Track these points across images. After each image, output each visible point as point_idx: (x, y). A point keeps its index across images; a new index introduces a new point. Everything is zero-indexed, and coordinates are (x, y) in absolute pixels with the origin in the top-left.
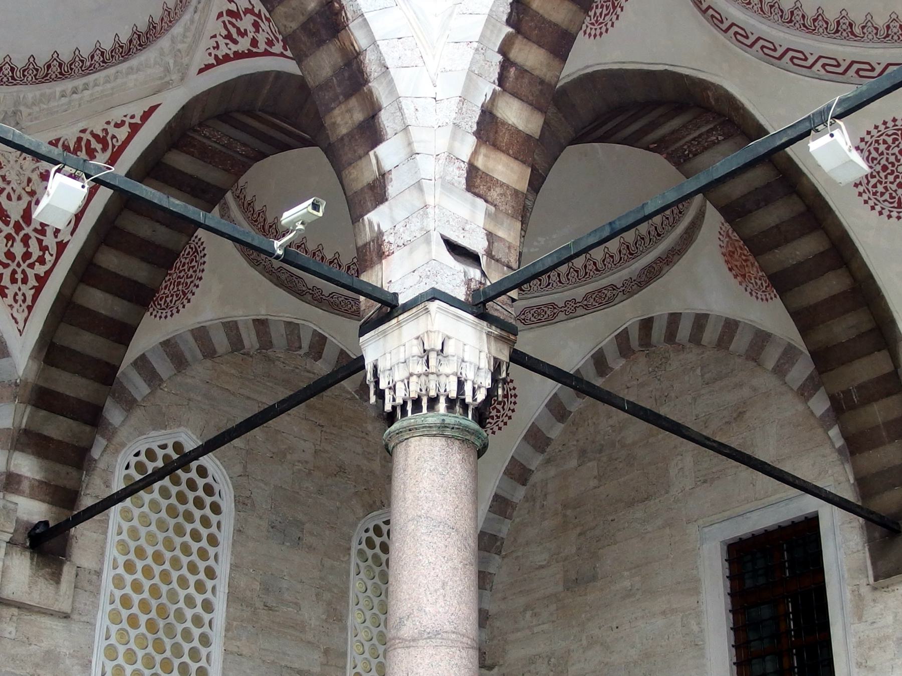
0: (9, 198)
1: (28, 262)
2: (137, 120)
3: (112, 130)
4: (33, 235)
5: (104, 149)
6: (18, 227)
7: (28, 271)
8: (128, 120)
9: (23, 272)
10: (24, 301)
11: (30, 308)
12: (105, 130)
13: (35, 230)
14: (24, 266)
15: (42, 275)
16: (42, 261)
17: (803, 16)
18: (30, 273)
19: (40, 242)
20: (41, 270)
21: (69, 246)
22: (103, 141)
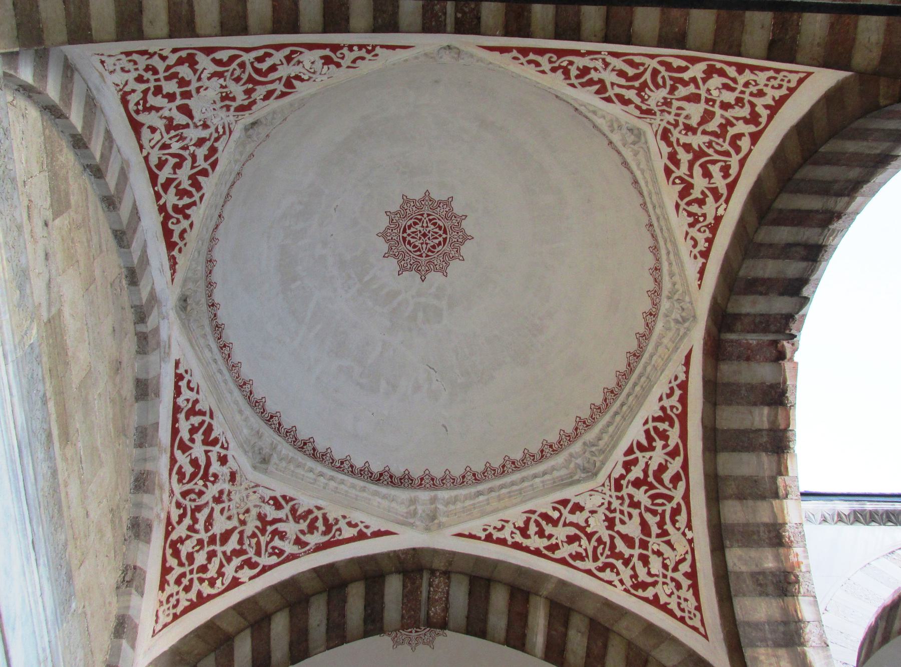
1: (200, 575)
3: (342, 524)
4: (220, 555)
5: (325, 533)
6: (212, 540)
7: (196, 582)
8: (361, 526)
9: (191, 581)
10: (175, 607)
11: (176, 617)
12: (337, 521)
13: (224, 553)
14: (195, 576)
18: (196, 586)
19: (222, 565)
20: (207, 590)
21: (241, 587)
22: (328, 527)
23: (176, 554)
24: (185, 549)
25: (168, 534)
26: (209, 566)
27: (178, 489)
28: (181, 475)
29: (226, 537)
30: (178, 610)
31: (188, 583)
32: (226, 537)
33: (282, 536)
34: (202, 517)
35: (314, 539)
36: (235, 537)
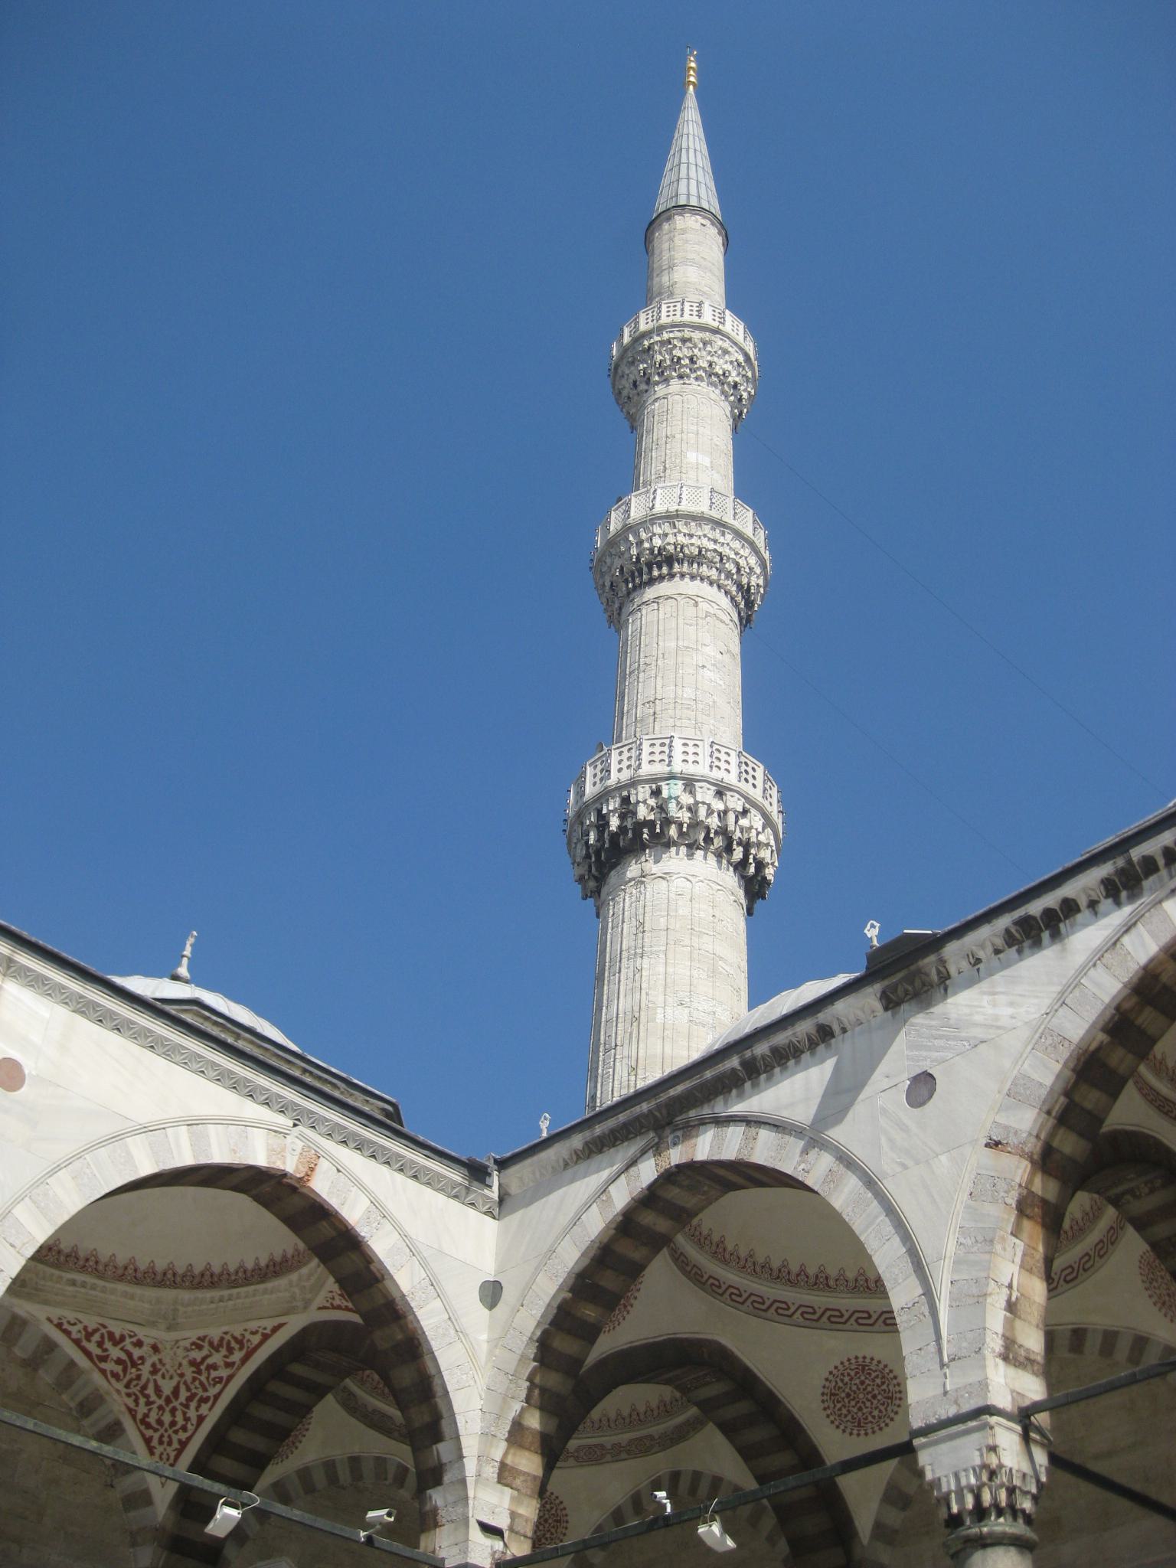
0: (163, 1377)
3: (248, 1336)
5: (241, 1349)
6: (168, 1401)
9: (169, 1436)
14: (170, 1432)
16: (184, 1429)
18: (175, 1438)
19: (184, 1414)
20: (183, 1436)
21: (208, 1419)
22: (240, 1343)
23: (148, 1426)
24: (152, 1420)
25: (134, 1417)
27: (120, 1386)
28: (115, 1376)
32: (176, 1392)
33: (214, 1367)
34: (150, 1390)
35: (237, 1356)
36: (183, 1388)
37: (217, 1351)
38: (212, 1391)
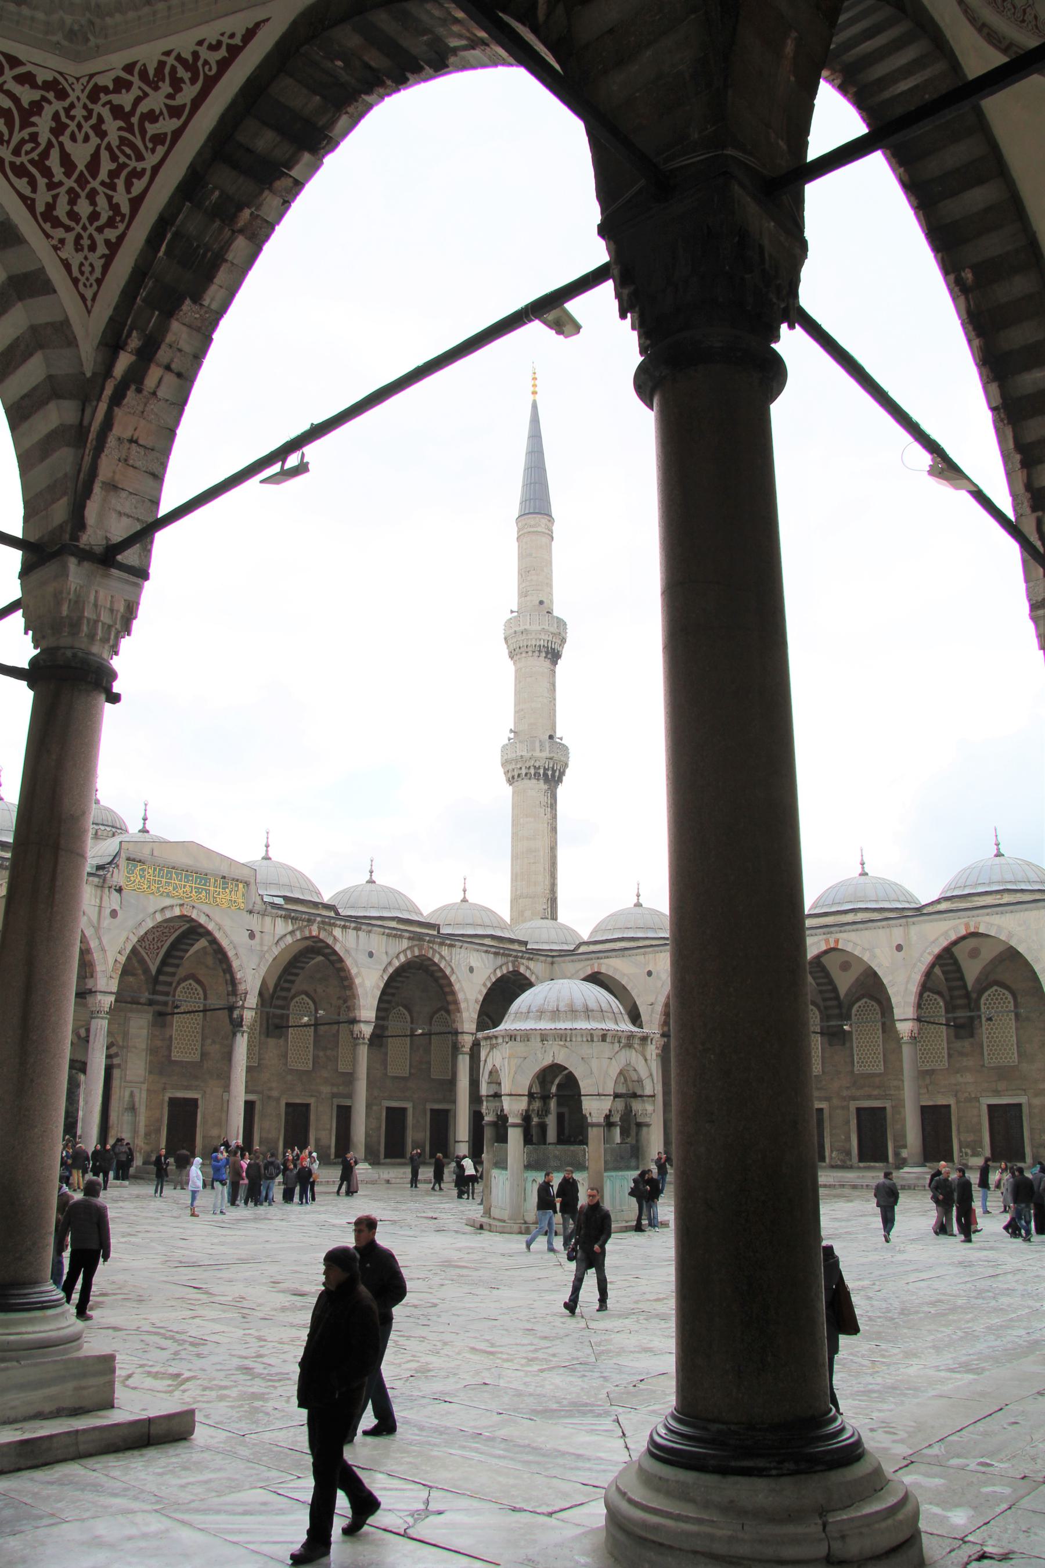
0: (73, 138)
2: (237, 41)
3: (204, 53)
5: (193, 81)
6: (82, 181)
8: (225, 40)
11: (99, 282)
12: (196, 55)
13: (103, 184)
14: (91, 230)
15: (114, 240)
16: (111, 223)
17: (1036, 17)
18: (100, 239)
19: (109, 198)
20: (111, 234)
23: (56, 223)
26: (98, 209)
29: (94, 165)
30: (98, 273)
31: (89, 242)
32: (94, 165)
33: (152, 117)
34: (54, 162)
35: (188, 93)
36: (105, 155)
37: (156, 88)
38: (151, 160)
